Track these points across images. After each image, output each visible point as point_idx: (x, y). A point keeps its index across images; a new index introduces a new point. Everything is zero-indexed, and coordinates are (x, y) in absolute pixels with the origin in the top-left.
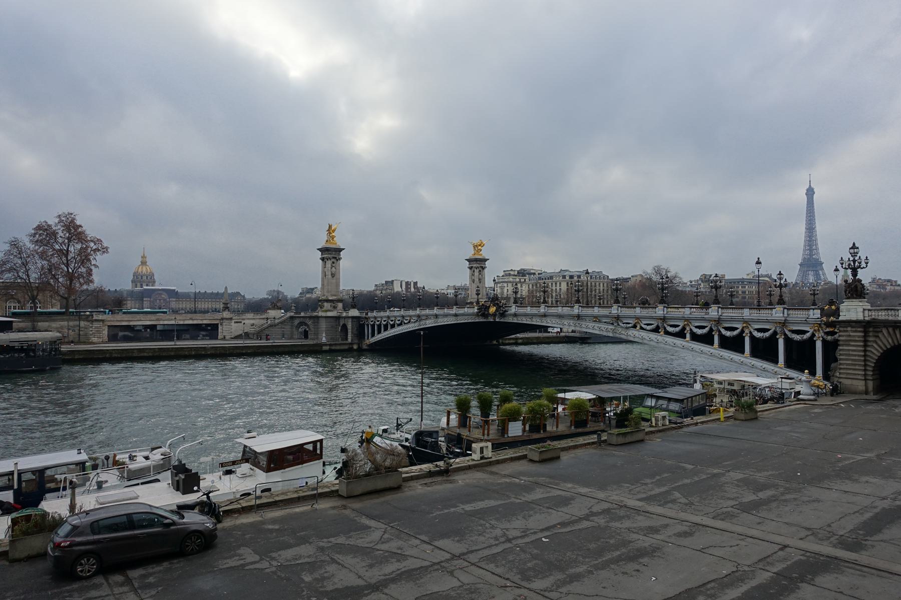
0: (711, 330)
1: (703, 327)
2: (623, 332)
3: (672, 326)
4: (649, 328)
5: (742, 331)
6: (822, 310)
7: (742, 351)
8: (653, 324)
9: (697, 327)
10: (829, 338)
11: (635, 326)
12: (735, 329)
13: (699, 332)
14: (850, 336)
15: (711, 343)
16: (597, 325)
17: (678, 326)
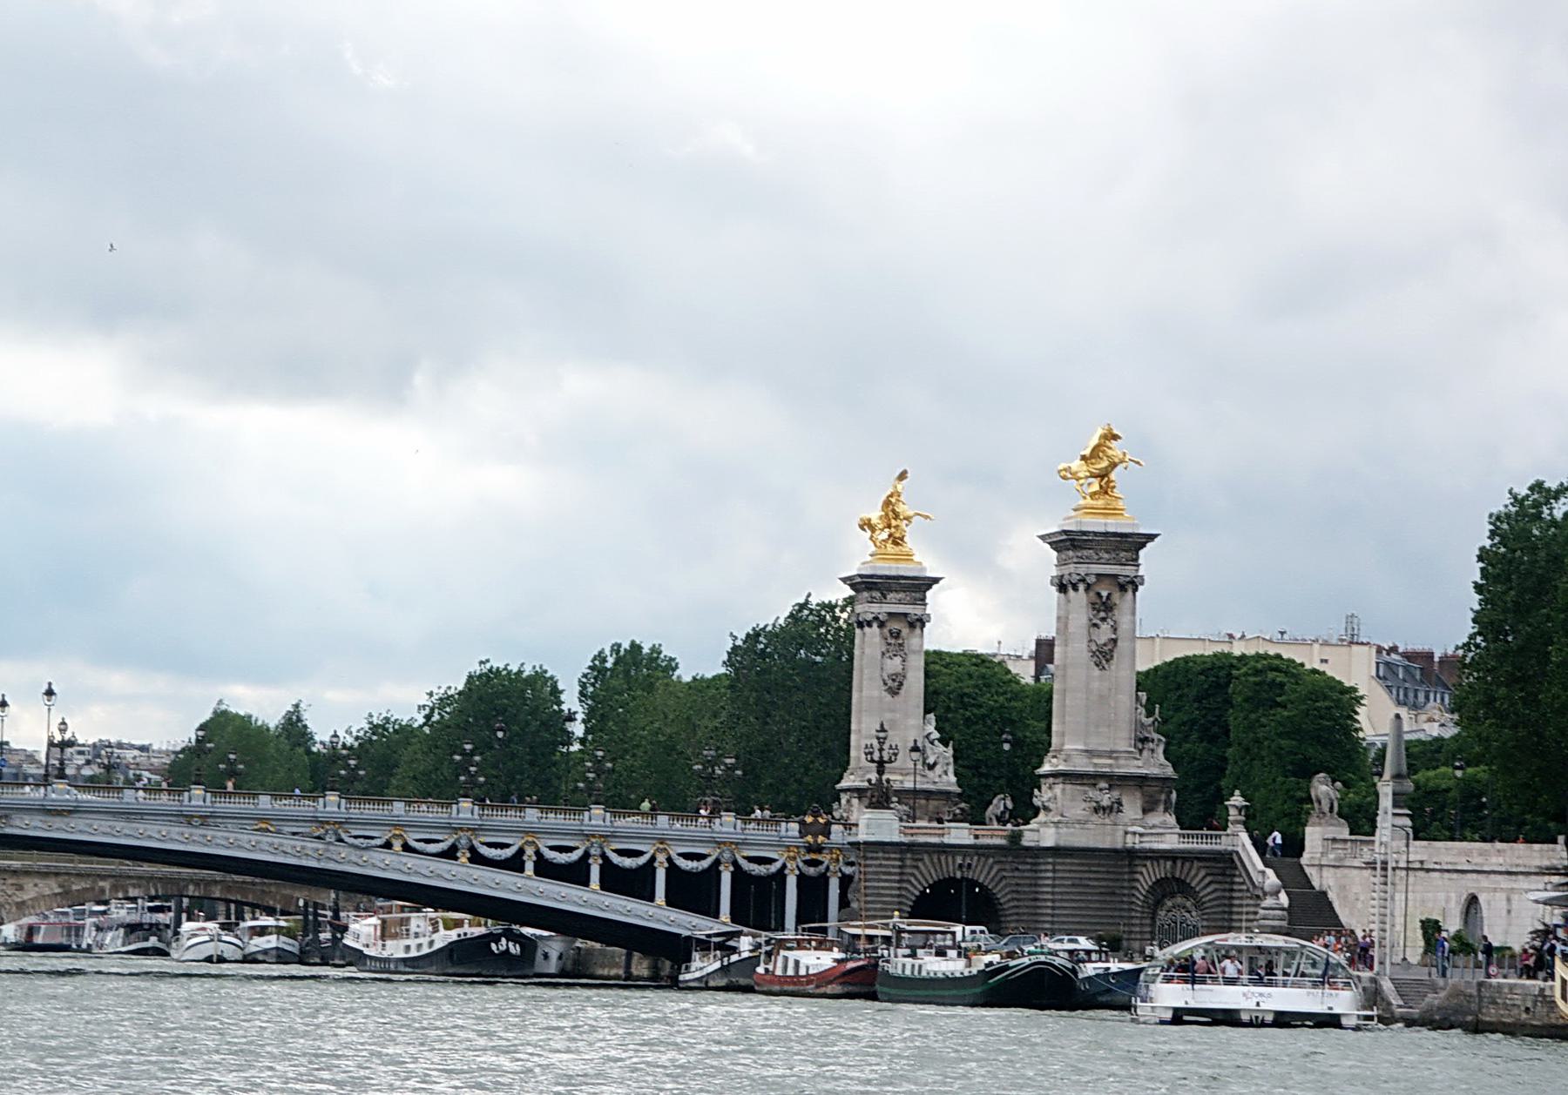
0: (587, 855)
2: (354, 858)
3: (490, 845)
4: (432, 848)
5: (653, 859)
6: (802, 823)
7: (650, 897)
8: (437, 841)
9: (552, 848)
10: (811, 871)
11: (388, 845)
12: (639, 854)
13: (562, 858)
14: (880, 865)
15: (584, 881)
16: (266, 839)
17: (507, 846)
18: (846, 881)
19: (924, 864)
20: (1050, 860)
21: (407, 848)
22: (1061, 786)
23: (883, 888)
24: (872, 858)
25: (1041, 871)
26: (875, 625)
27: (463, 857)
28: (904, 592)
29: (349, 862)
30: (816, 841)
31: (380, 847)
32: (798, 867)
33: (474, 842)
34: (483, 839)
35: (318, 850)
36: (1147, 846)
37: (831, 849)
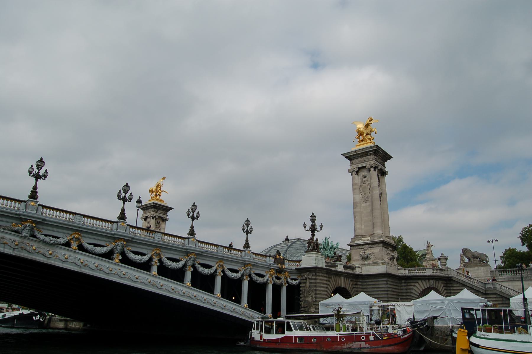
0: (185, 265)
1: (177, 261)
2: (42, 251)
4: (98, 250)
10: (278, 282)
11: (68, 244)
12: (209, 267)
14: (321, 279)
17: (143, 254)
18: (290, 288)
19: (332, 280)
20: (385, 279)
21: (81, 248)
22: (381, 248)
23: (322, 291)
24: (319, 276)
25: (368, 285)
26: (154, 219)
27: (117, 258)
28: (163, 211)
29: (39, 253)
30: (282, 267)
31: (63, 245)
32: (272, 280)
33: (126, 250)
34: (130, 248)
35: (15, 241)
36: (417, 274)
37: (285, 272)
